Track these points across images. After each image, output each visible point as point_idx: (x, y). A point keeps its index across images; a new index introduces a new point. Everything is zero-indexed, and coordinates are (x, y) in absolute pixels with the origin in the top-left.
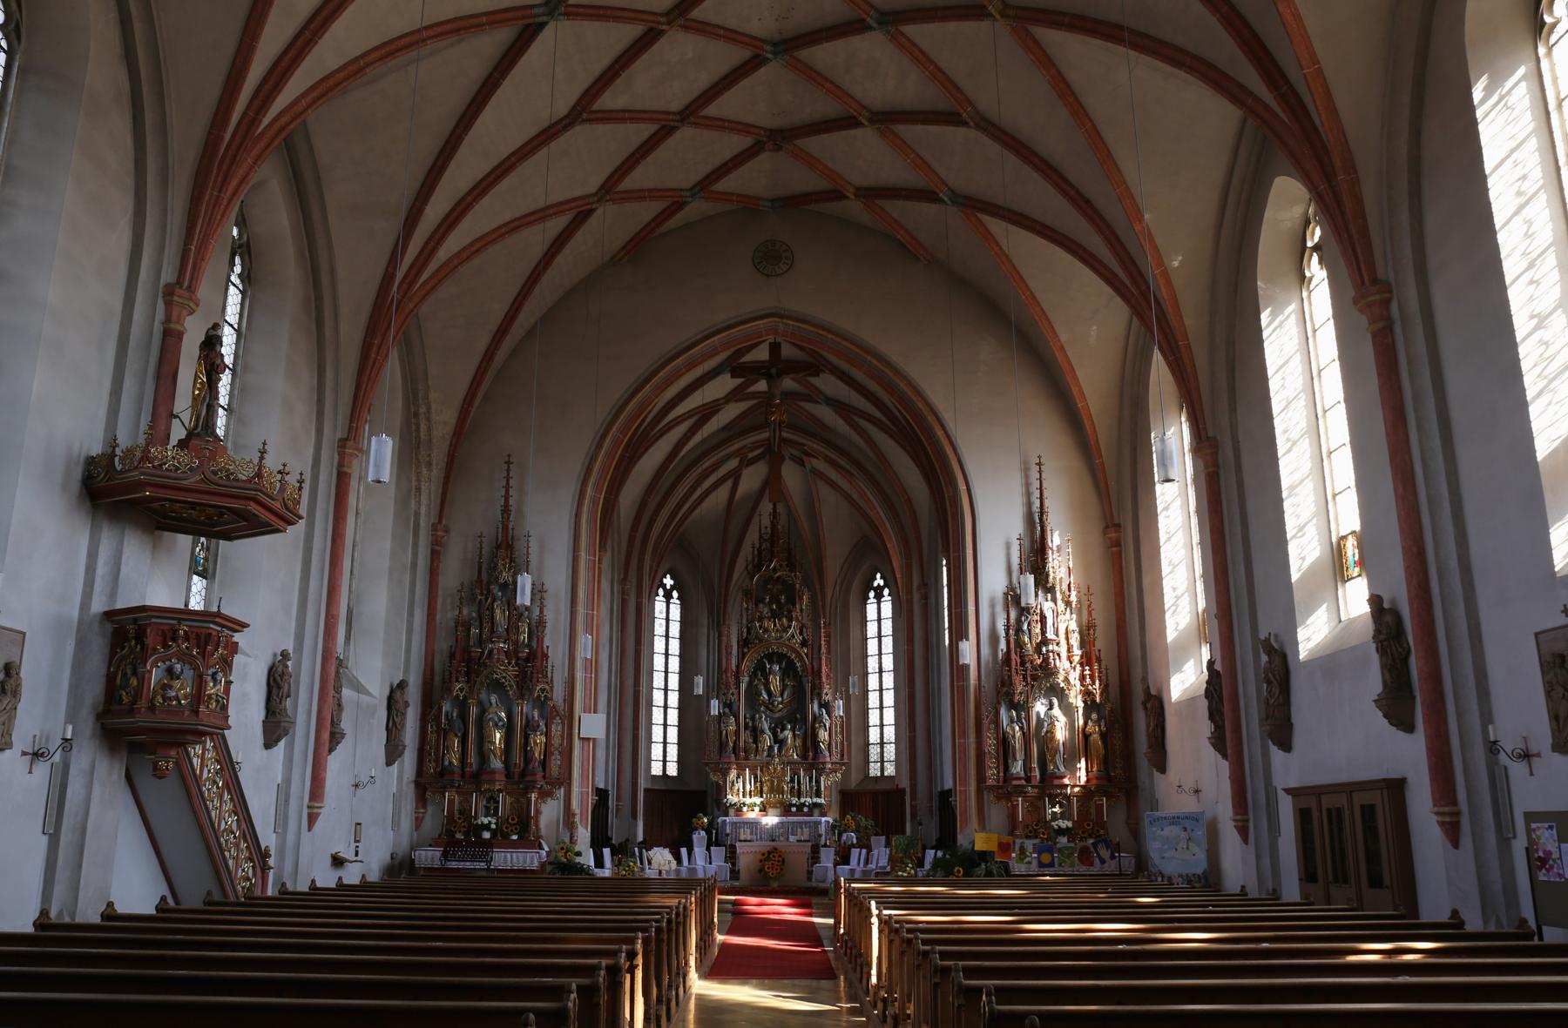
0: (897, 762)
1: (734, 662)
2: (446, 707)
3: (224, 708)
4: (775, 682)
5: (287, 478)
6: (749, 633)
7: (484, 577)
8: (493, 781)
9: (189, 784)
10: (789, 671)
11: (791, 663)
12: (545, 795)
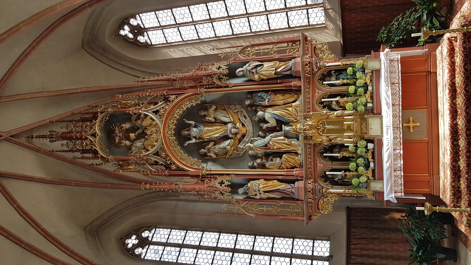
6: (156, 163)
10: (197, 114)
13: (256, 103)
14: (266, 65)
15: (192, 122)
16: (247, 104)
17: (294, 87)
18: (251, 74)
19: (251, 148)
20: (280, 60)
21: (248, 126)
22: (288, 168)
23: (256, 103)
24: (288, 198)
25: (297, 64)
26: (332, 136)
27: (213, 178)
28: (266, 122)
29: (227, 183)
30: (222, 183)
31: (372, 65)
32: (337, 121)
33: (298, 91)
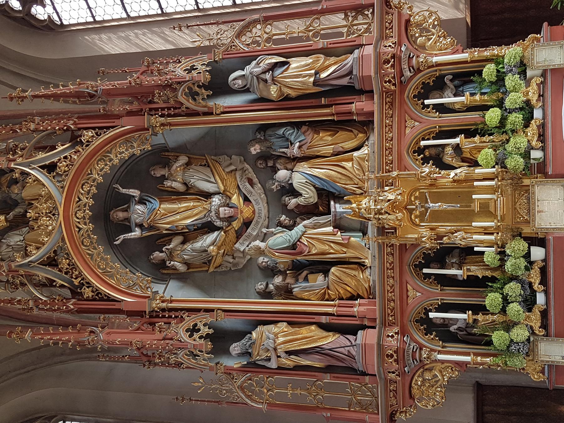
13: (275, 150)
14: (296, 63)
15: (135, 193)
16: (254, 152)
17: (358, 114)
18: (262, 84)
19: (260, 252)
20: (327, 52)
21: (258, 203)
22: (341, 299)
23: (275, 150)
24: (341, 368)
26: (444, 227)
27: (176, 317)
28: (295, 194)
29: (205, 330)
30: (194, 330)
32: (456, 193)
33: (365, 124)
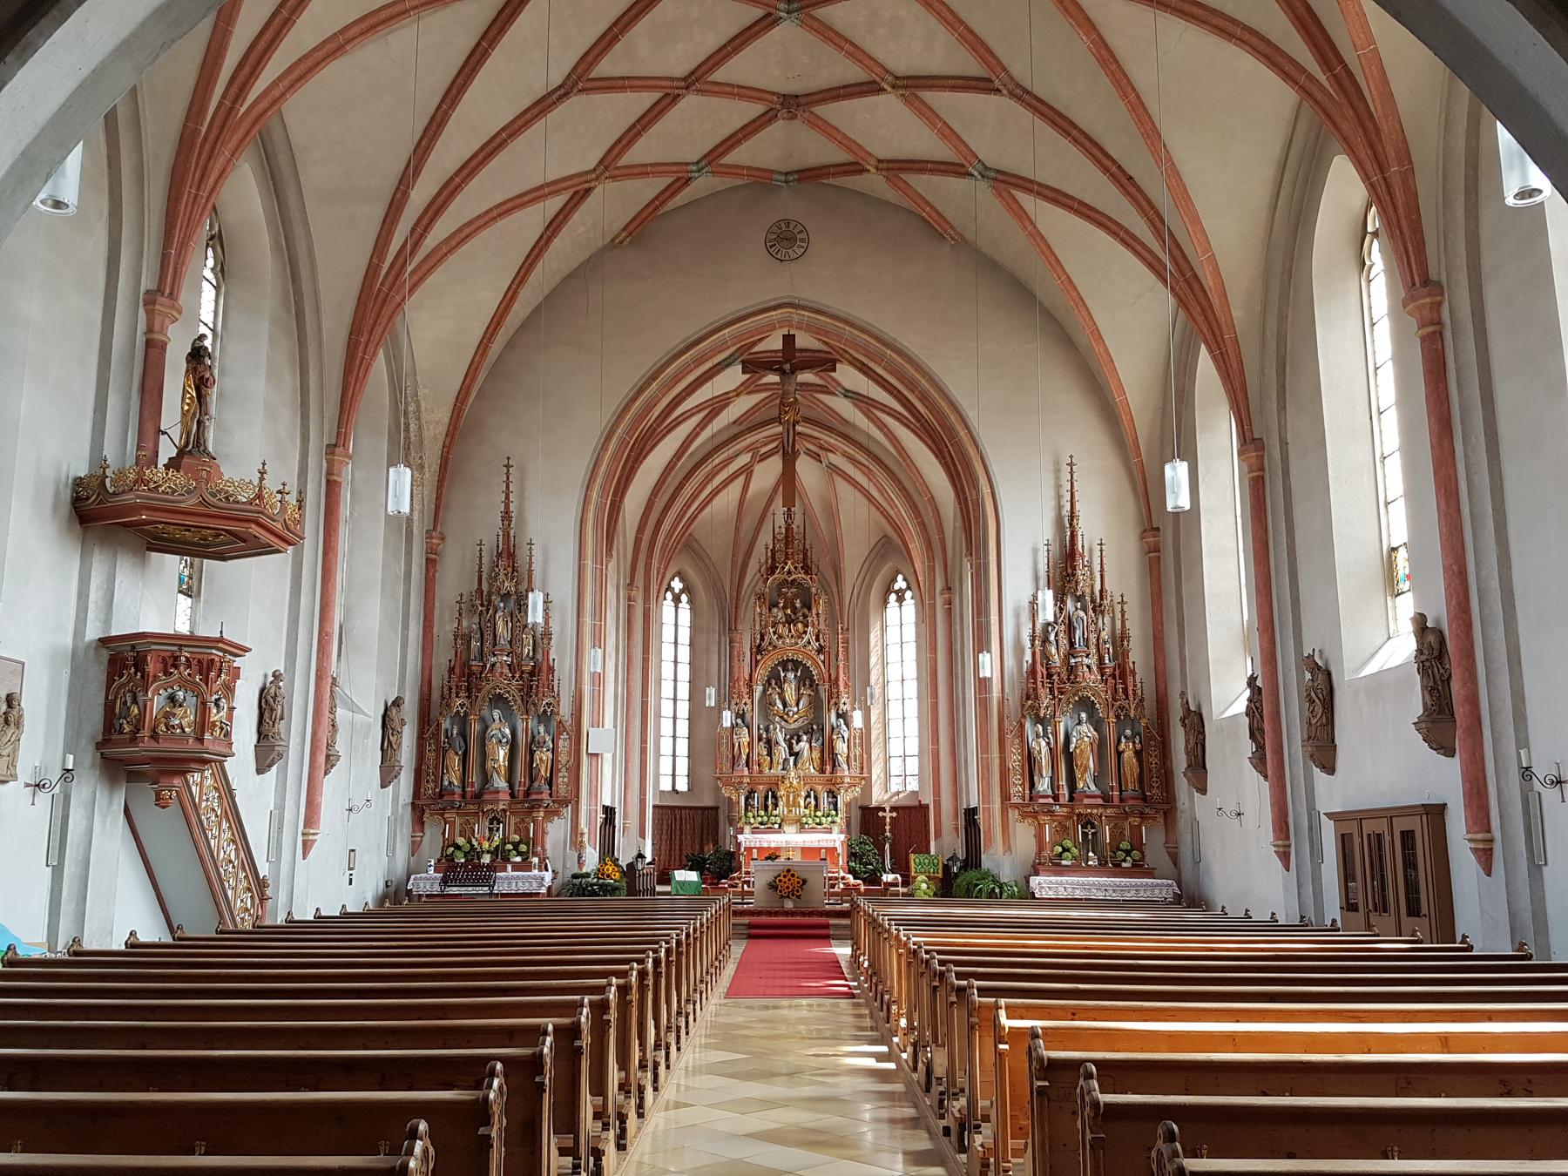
0: (921, 776)
1: (747, 671)
2: (446, 724)
3: (228, 734)
4: (790, 692)
5: (287, 498)
6: (762, 639)
7: (485, 587)
8: (497, 801)
9: (189, 813)
10: (806, 679)
11: (806, 669)
12: (552, 813)
24: (734, 761)
25: (844, 771)
31: (836, 829)
33: (822, 771)
